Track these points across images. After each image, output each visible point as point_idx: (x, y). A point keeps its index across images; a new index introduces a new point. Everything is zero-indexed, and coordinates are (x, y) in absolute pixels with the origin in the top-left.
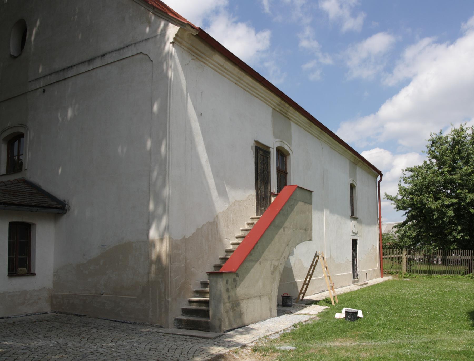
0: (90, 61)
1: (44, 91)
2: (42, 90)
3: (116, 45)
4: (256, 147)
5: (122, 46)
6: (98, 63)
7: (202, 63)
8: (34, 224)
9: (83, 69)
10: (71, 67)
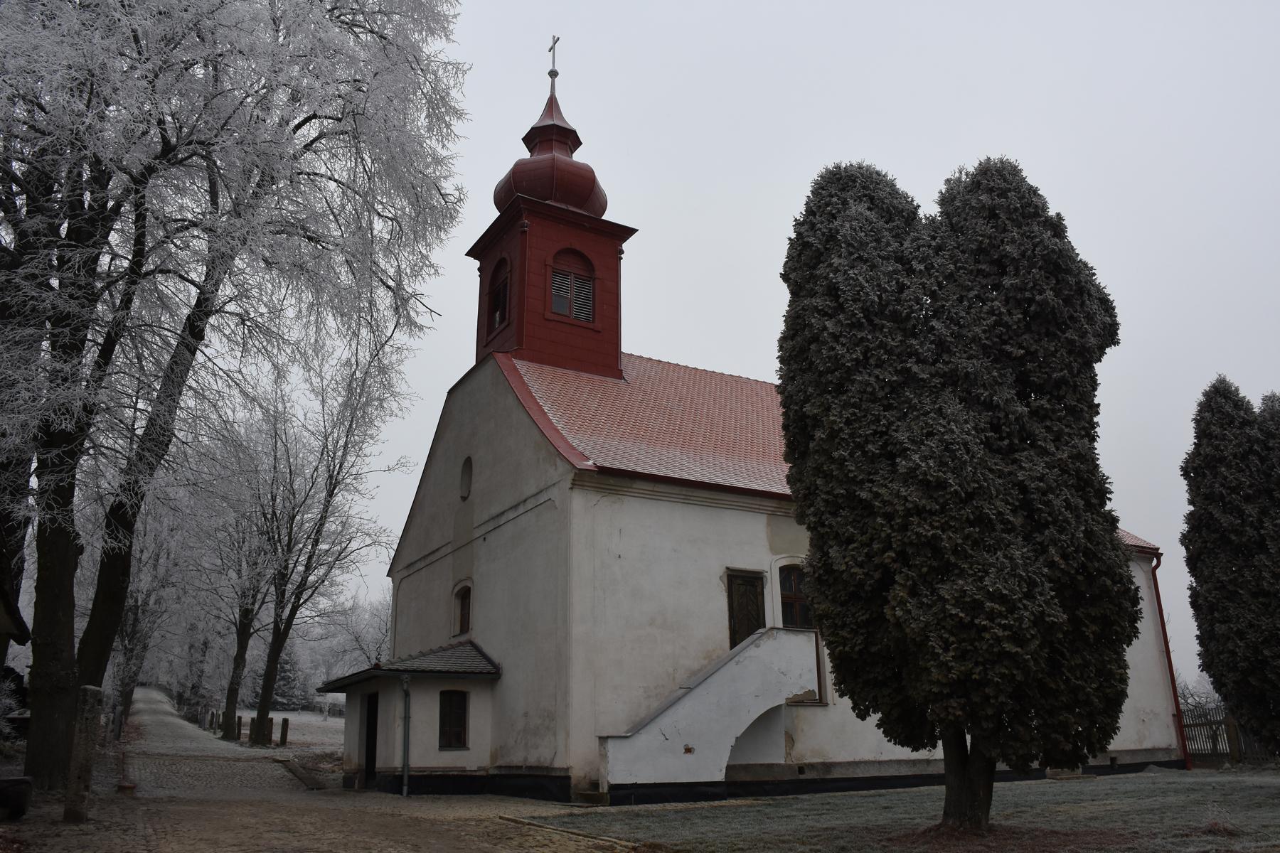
0: (515, 507)
1: (485, 539)
2: (482, 539)
3: (533, 490)
4: (728, 576)
5: (537, 491)
6: (521, 509)
7: (620, 496)
8: (468, 692)
9: (511, 515)
10: (503, 513)
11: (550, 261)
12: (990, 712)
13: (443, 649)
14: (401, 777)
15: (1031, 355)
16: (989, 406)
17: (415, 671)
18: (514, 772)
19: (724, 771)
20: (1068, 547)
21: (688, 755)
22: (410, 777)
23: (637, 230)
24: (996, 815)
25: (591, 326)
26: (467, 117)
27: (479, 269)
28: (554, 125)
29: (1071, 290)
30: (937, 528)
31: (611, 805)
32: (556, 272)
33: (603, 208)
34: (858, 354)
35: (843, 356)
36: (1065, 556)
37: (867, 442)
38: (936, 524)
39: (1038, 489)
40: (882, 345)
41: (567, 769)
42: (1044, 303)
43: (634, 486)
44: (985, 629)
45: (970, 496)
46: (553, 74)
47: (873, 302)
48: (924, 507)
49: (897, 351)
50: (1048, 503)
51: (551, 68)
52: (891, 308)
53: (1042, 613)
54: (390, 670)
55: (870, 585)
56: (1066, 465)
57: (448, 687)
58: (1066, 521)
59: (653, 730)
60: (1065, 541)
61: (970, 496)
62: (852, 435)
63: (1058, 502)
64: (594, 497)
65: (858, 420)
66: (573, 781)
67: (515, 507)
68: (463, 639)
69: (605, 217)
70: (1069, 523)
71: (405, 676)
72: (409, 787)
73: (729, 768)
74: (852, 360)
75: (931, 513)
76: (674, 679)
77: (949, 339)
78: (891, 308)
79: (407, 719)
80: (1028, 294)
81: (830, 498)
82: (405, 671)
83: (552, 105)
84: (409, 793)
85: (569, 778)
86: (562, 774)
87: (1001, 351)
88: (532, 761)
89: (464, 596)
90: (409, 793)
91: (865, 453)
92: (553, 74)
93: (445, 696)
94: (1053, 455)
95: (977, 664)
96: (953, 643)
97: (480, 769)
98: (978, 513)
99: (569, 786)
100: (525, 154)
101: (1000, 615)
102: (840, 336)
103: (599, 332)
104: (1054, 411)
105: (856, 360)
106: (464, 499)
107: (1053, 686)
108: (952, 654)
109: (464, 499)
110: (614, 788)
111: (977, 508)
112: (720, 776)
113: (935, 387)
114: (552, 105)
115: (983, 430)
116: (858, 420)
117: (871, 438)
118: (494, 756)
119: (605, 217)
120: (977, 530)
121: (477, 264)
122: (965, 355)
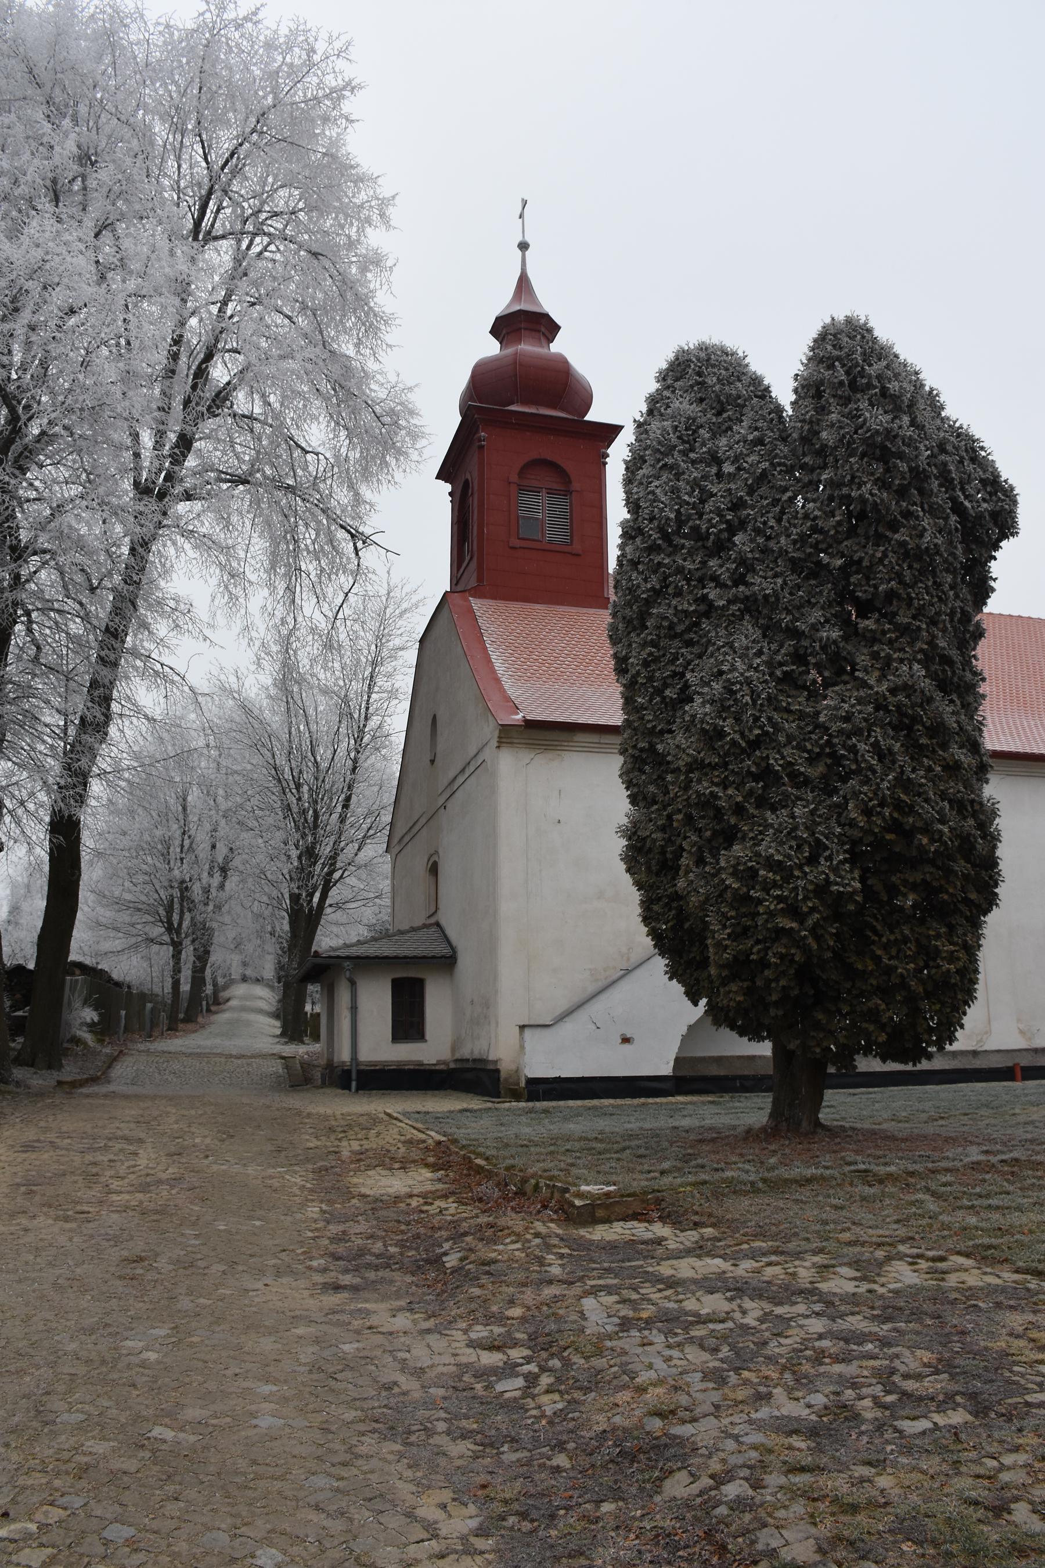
11: (514, 478)
12: (774, 997)
13: (414, 929)
14: (348, 1072)
15: (852, 565)
16: (793, 633)
17: (358, 957)
18: (470, 1065)
19: (672, 1063)
20: (871, 800)
21: (626, 1046)
22: (360, 1072)
23: (622, 427)
24: (824, 1116)
25: (568, 549)
26: (397, 322)
27: (450, 494)
28: (520, 311)
29: (904, 478)
30: (717, 785)
31: (528, 1101)
32: (521, 488)
33: (586, 401)
34: (654, 581)
35: (638, 586)
36: (867, 812)
37: (666, 686)
38: (716, 780)
39: (841, 731)
40: (680, 570)
41: (496, 1062)
42: (862, 500)
43: (576, 738)
44: (760, 902)
45: (755, 744)
46: (523, 246)
47: (668, 519)
48: (703, 761)
49: (699, 574)
50: (853, 749)
51: (520, 239)
52: (690, 523)
53: (827, 880)
54: (330, 957)
55: (672, 852)
56: (885, 699)
57: (399, 975)
58: (871, 769)
59: (582, 1016)
60: (865, 794)
61: (755, 744)
62: (650, 679)
63: (862, 747)
64: (525, 756)
65: (656, 660)
66: (503, 1075)
67: (463, 770)
68: (432, 920)
69: (589, 417)
70: (874, 772)
71: (346, 964)
72: (358, 1080)
73: (677, 1060)
74: (648, 590)
75: (713, 767)
76: (628, 959)
77: (750, 555)
78: (690, 523)
79: (354, 1009)
80: (845, 490)
81: (637, 753)
82: (348, 958)
83: (523, 284)
84: (358, 1089)
85: (498, 1071)
86: (491, 1067)
87: (819, 563)
88: (476, 1055)
89: (434, 870)
90: (358, 1089)
91: (664, 698)
92: (523, 246)
93: (398, 986)
94: (871, 688)
95: (758, 942)
96: (732, 917)
97: (439, 1063)
98: (763, 764)
99: (499, 1079)
100: (492, 348)
101: (775, 885)
102: (639, 563)
103: (578, 555)
104: (884, 633)
105: (653, 589)
106: (432, 762)
107: (860, 967)
108: (728, 931)
109: (432, 762)
110: (532, 1082)
111: (762, 758)
112: (666, 1069)
113: (733, 615)
114: (523, 284)
115: (781, 664)
116: (656, 660)
117: (669, 681)
118: (453, 1049)
119: (589, 417)
120: (761, 784)
121: (448, 487)
122: (770, 574)
